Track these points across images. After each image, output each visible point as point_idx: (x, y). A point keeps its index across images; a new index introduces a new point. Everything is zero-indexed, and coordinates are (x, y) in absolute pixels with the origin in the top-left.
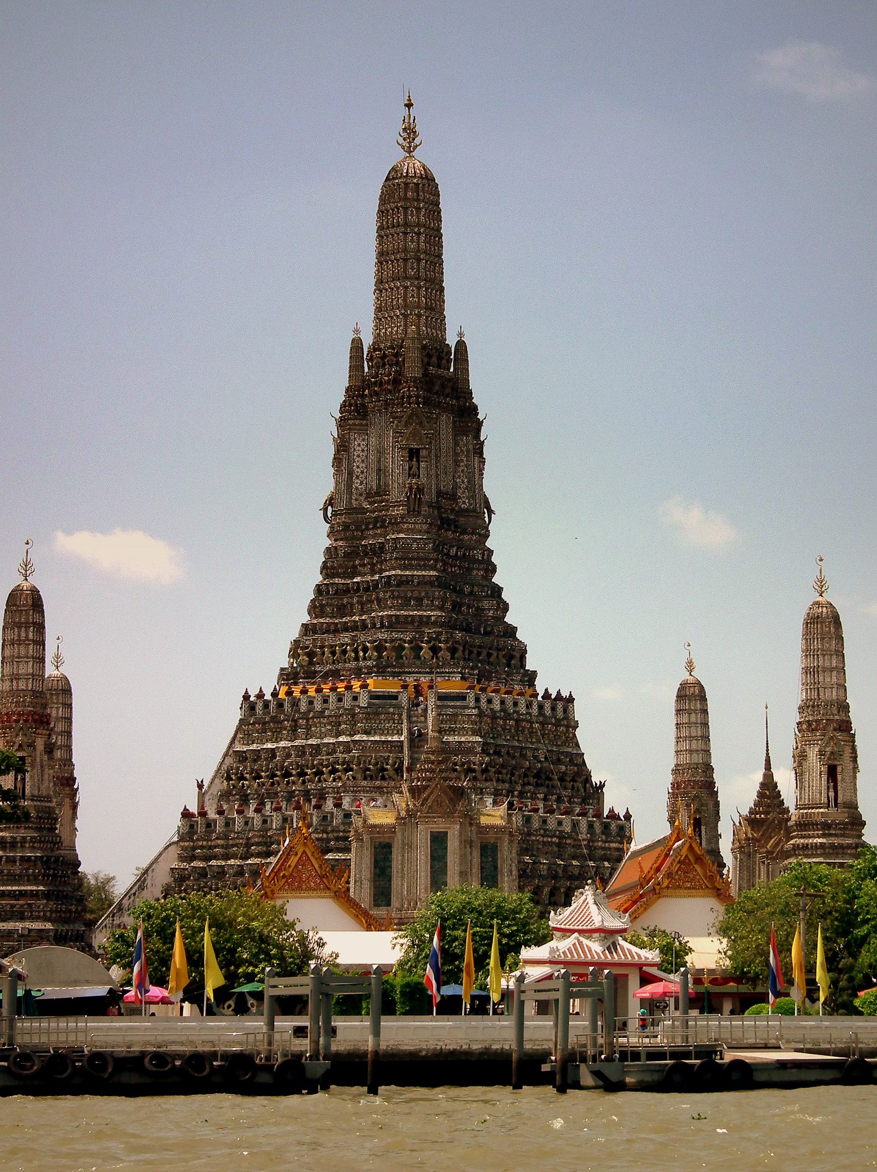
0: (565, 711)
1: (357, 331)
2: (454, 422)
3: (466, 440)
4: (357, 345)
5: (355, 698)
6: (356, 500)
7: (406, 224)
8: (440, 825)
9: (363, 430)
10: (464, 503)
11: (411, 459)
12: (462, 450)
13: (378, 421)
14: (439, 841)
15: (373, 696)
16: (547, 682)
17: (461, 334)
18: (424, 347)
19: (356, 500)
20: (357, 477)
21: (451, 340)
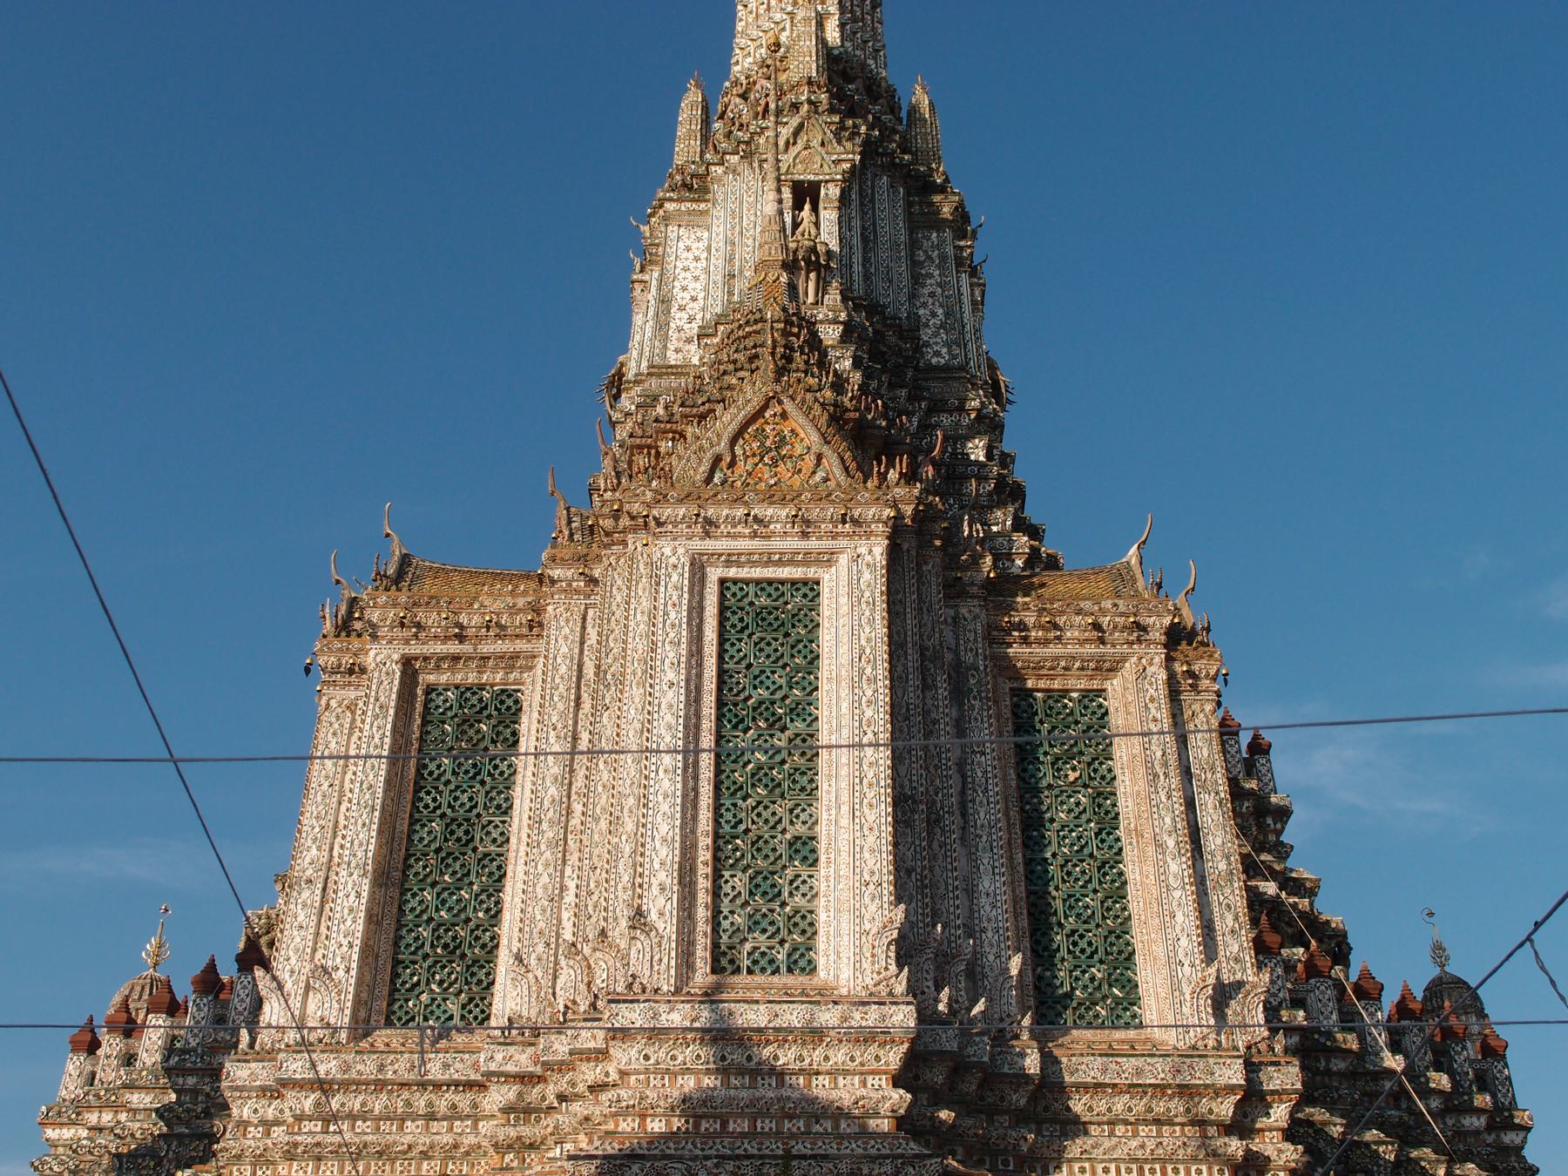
2: (910, 204)
6: (677, 351)
10: (937, 353)
12: (929, 258)
19: (677, 351)
20: (682, 308)
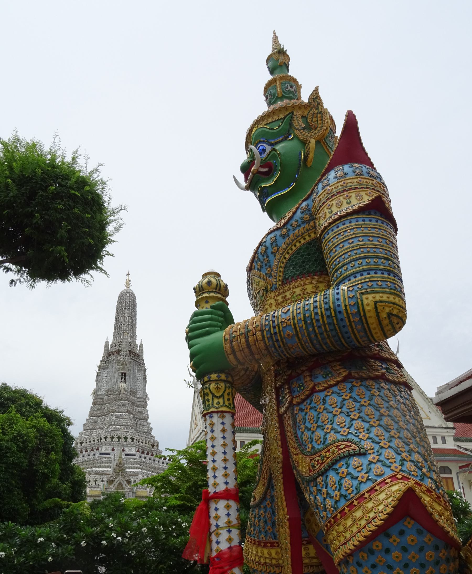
4: (107, 343)
9: (107, 368)
11: (122, 375)
21: (138, 343)
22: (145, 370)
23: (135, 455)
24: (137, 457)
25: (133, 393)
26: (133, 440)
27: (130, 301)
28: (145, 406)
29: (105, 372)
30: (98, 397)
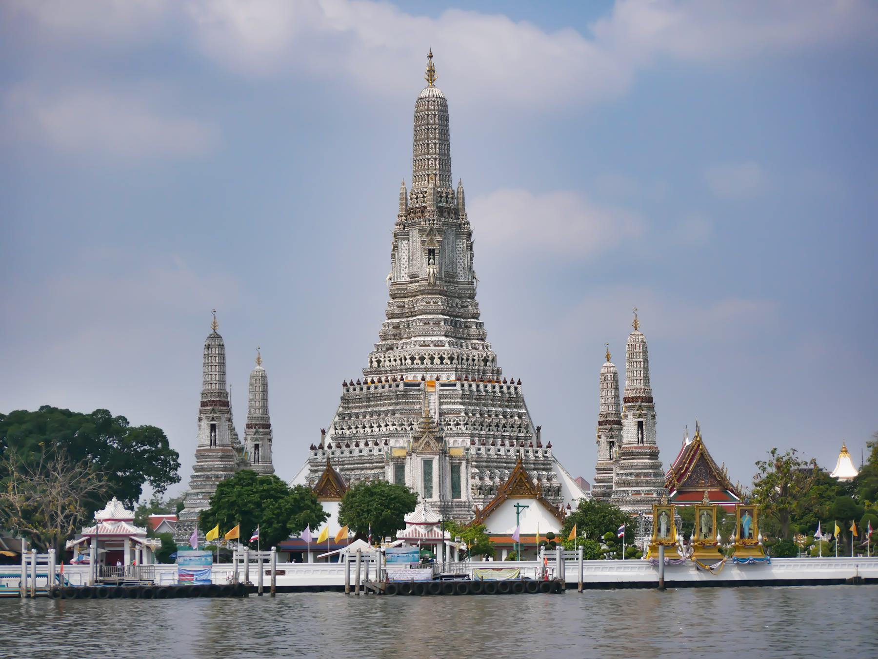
0: (516, 389)
1: (403, 184)
3: (463, 243)
5: (398, 386)
7: (428, 124)
8: (428, 456)
9: (406, 236)
11: (430, 255)
13: (414, 234)
14: (428, 464)
15: (406, 385)
16: (506, 375)
17: (460, 183)
18: (438, 193)
21: (455, 186)
22: (469, 234)
23: (455, 385)
24: (458, 387)
25: (450, 278)
26: (451, 359)
27: (435, 115)
28: (472, 296)
29: (403, 245)
30: (398, 286)
